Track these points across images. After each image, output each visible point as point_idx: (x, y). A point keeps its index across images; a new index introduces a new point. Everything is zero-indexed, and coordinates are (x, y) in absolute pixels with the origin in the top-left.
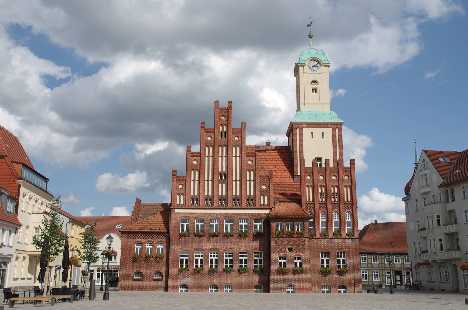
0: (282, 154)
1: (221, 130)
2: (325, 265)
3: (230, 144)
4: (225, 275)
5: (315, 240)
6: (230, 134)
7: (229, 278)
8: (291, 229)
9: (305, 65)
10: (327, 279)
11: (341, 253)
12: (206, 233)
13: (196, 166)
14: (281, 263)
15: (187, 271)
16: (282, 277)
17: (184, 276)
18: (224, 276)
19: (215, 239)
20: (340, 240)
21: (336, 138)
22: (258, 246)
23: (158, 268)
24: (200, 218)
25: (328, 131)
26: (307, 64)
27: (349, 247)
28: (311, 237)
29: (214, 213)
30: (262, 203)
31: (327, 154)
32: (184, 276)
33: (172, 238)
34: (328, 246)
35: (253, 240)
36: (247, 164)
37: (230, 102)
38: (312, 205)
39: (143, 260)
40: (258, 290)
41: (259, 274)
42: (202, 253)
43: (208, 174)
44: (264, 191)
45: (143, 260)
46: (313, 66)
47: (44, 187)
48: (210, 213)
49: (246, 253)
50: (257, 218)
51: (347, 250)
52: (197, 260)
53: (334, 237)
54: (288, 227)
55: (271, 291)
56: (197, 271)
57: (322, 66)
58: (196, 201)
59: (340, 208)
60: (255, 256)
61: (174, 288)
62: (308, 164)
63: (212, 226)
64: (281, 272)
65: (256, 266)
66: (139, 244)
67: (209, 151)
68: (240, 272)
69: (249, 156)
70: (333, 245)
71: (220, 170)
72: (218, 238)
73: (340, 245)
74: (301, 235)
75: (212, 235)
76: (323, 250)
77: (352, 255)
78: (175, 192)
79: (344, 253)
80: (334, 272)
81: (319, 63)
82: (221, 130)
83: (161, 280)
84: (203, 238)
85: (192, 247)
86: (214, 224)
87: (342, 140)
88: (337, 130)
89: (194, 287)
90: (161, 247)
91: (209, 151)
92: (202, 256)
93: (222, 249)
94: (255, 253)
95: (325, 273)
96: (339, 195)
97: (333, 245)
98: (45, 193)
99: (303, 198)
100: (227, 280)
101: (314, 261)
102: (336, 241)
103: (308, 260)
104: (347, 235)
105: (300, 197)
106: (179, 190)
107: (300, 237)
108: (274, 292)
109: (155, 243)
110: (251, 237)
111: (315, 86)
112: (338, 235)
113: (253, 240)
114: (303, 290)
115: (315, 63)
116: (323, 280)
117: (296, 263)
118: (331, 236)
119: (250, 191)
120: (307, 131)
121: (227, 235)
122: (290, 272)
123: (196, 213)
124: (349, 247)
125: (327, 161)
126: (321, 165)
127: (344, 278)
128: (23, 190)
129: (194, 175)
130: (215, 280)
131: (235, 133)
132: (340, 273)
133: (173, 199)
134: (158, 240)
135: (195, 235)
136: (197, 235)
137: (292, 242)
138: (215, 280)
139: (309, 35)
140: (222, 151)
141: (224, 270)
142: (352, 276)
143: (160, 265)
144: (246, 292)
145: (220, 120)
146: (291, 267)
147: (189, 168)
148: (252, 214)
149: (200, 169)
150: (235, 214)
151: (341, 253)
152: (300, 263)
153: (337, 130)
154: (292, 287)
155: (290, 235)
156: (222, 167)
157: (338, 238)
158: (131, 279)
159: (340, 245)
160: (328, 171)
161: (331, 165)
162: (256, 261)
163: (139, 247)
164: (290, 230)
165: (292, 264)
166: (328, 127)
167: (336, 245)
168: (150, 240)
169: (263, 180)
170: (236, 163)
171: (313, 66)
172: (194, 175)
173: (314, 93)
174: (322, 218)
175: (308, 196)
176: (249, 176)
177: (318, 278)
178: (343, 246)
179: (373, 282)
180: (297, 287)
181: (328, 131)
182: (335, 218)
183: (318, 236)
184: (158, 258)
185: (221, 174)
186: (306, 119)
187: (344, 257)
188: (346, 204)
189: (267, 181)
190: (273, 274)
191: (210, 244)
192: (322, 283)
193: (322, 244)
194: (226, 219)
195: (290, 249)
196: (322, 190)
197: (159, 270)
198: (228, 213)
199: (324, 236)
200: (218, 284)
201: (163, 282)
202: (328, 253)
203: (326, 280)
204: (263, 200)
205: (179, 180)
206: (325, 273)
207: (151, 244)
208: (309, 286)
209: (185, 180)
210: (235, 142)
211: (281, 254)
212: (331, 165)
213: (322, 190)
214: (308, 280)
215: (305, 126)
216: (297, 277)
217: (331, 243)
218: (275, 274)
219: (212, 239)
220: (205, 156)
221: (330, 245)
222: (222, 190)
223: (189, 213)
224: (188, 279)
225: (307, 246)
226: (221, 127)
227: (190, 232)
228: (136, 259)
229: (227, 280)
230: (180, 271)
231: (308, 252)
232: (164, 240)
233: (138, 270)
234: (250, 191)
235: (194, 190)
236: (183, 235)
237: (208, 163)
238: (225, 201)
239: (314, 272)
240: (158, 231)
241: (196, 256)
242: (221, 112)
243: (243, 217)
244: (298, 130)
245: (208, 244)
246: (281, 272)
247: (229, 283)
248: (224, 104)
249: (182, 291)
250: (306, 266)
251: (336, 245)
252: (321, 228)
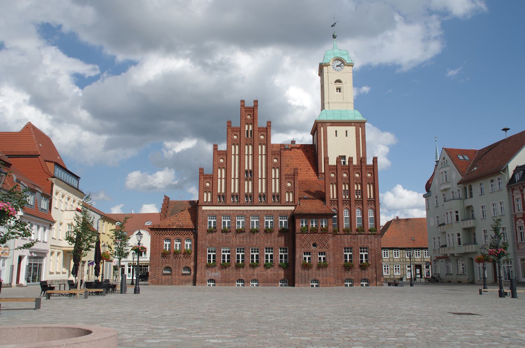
0: (307, 152)
1: (247, 129)
2: (348, 260)
3: (256, 143)
4: (252, 270)
5: (339, 236)
6: (256, 133)
7: (255, 272)
8: (316, 226)
9: (329, 65)
10: (350, 273)
11: (364, 248)
12: (232, 229)
13: (222, 164)
14: (305, 258)
15: (214, 266)
16: (306, 272)
17: (212, 271)
18: (250, 271)
19: (241, 235)
20: (363, 236)
21: (359, 136)
22: (283, 242)
23: (186, 263)
24: (227, 215)
25: (352, 130)
26: (331, 63)
27: (371, 243)
28: (335, 233)
29: (240, 210)
30: (287, 200)
31: (350, 151)
32: (212, 271)
33: (199, 234)
34: (351, 242)
35: (278, 236)
36: (272, 162)
37: (256, 102)
38: (336, 202)
39: (171, 256)
40: (284, 284)
41: (284, 269)
42: (229, 248)
43: (235, 172)
44: (289, 188)
45: (171, 256)
46: (337, 66)
47: (76, 186)
48: (237, 210)
49: (272, 249)
50: (282, 214)
51: (369, 245)
52: (224, 256)
53: (357, 233)
54: (312, 223)
55: (296, 285)
56: (224, 266)
57: (346, 65)
58: (223, 199)
59: (362, 205)
60: (281, 252)
61: (202, 283)
62: (332, 162)
63: (239, 222)
64: (306, 266)
65: (281, 261)
66: (168, 240)
67: (235, 150)
68: (267, 267)
69: (275, 155)
70: (356, 241)
71: (246, 168)
72: (244, 234)
73: (363, 241)
74: (325, 231)
75: (239, 231)
76: (347, 245)
77: (374, 250)
78: (203, 190)
79: (366, 248)
80: (357, 266)
81: (343, 62)
82: (247, 129)
83: (190, 275)
84: (230, 234)
85: (219, 243)
86: (241, 221)
87: (365, 138)
88: (360, 129)
89: (222, 282)
90: (189, 243)
91: (235, 150)
92: (229, 252)
93: (248, 245)
94: (281, 249)
95: (348, 267)
96: (362, 192)
97: (356, 241)
98: (77, 191)
99: (327, 195)
100: (254, 275)
101: (338, 256)
102: (359, 236)
103: (331, 255)
104: (370, 231)
105: (324, 194)
106: (206, 188)
107: (324, 233)
108: (298, 286)
109: (183, 239)
110: (276, 233)
111: (339, 85)
112: (361, 230)
113: (278, 236)
114: (326, 283)
115: (339, 63)
116: (346, 274)
117: (320, 258)
118: (354, 231)
119: (275, 188)
120: (331, 130)
121: (254, 232)
122: (315, 267)
123: (223, 210)
124: (371, 243)
125: (351, 159)
126: (344, 163)
127: (367, 272)
128: (56, 188)
129: (221, 173)
130: (241, 275)
131: (261, 131)
132: (363, 267)
133: (201, 196)
134: (186, 236)
135: (222, 232)
136: (224, 231)
137: (316, 238)
138: (241, 275)
139: (333, 36)
140: (248, 150)
141: (250, 266)
142: (374, 270)
143: (188, 260)
144: (272, 286)
145: (246, 119)
146: (315, 262)
147: (216, 166)
148: (277, 210)
149: (227, 168)
150: (261, 211)
151: (364, 248)
152: (324, 258)
153: (360, 129)
154: (316, 281)
155: (314, 231)
156: (248, 165)
157: (361, 234)
158: (161, 274)
159: (363, 241)
160: (351, 169)
161: (355, 162)
162: (281, 256)
163: (168, 243)
164: (314, 226)
165: (317, 258)
166: (351, 126)
167: (359, 240)
168: (178, 236)
169: (289, 178)
170: (262, 161)
171: (337, 66)
172: (221, 173)
173: (338, 93)
174: (346, 214)
175: (332, 193)
176: (275, 173)
177: (341, 272)
178: (366, 241)
179: (394, 275)
180: (321, 281)
181: (352, 130)
182: (358, 215)
183: (341, 232)
184: (187, 254)
185: (247, 172)
186: (331, 118)
187: (366, 252)
188: (369, 201)
189: (292, 178)
190: (298, 269)
191: (236, 240)
193: (346, 240)
194: (251, 215)
195: (314, 245)
196: (345, 187)
197: (188, 265)
198: (254, 210)
199: (347, 232)
200: (244, 279)
201: (191, 277)
202: (351, 248)
203: (348, 275)
204: (288, 197)
205: (206, 178)
206: (348, 267)
207: (179, 240)
208: (332, 280)
209: (212, 178)
210: (261, 140)
211: (306, 249)
212: (355, 162)
213: (345, 187)
214: (332, 274)
215: (329, 124)
216: (321, 272)
217: (354, 239)
218: (300, 269)
219: (238, 235)
220: (231, 154)
221: (353, 241)
222: (248, 187)
223: (216, 210)
224: (216, 274)
225: (331, 241)
226: (247, 126)
227: (218, 228)
228: (165, 255)
229: (254, 275)
230: (208, 266)
231: (332, 247)
232: (192, 237)
233: (167, 265)
234: (275, 188)
235: (221, 188)
236: (210, 231)
237: (234, 161)
238: (251, 199)
240: (186, 227)
241: (223, 252)
242: (247, 111)
243: (269, 214)
244: (322, 129)
245: (235, 240)
246: (306, 266)
247: (255, 277)
248: (249, 104)
249: (210, 285)
250: (330, 260)
251: (359, 240)
252: (345, 224)
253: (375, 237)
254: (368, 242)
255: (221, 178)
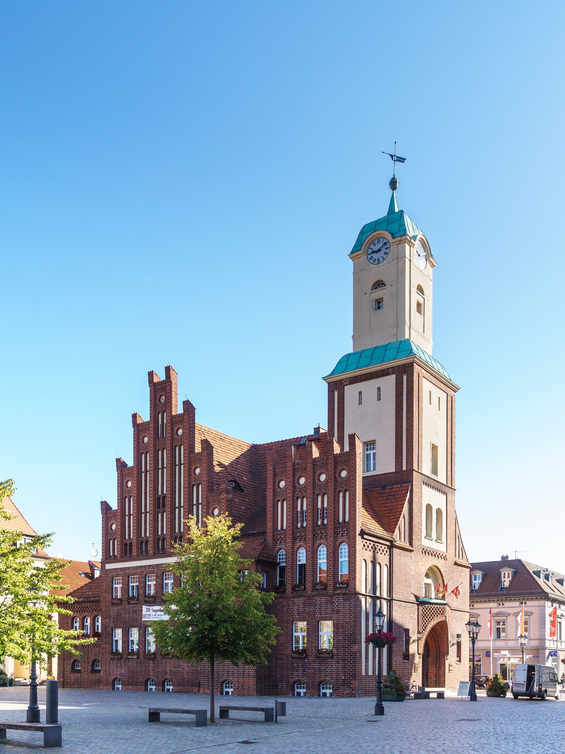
20: (324, 599)
34: (304, 611)
67: (147, 461)
73: (323, 609)
77: (343, 627)
100: (166, 673)
120: (350, 391)
124: (338, 612)
142: (340, 665)
175: (283, 521)
192: (293, 678)
193: (295, 608)
217: (310, 605)
229: (166, 673)
239: (282, 659)
251: (318, 607)
253: (345, 600)
254: (333, 610)
255: (130, 515)
